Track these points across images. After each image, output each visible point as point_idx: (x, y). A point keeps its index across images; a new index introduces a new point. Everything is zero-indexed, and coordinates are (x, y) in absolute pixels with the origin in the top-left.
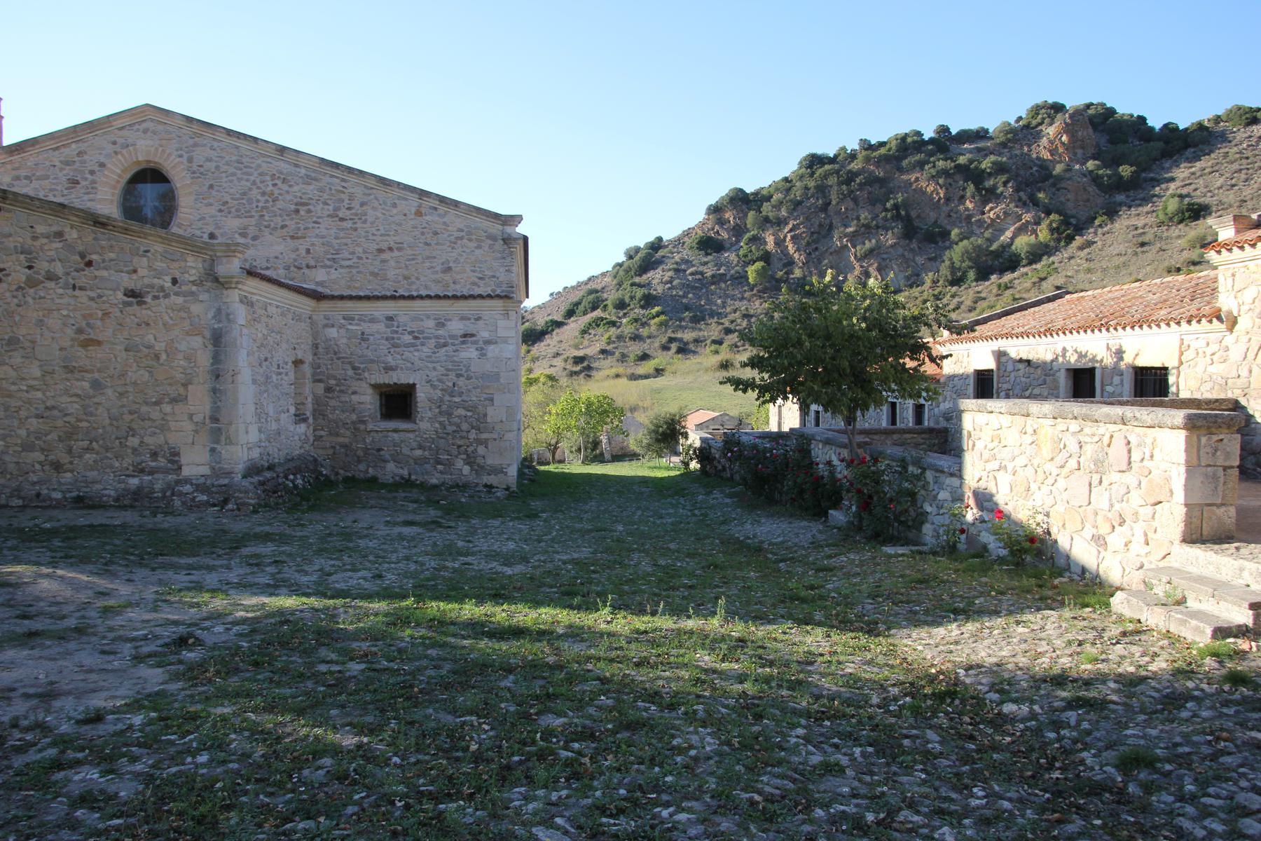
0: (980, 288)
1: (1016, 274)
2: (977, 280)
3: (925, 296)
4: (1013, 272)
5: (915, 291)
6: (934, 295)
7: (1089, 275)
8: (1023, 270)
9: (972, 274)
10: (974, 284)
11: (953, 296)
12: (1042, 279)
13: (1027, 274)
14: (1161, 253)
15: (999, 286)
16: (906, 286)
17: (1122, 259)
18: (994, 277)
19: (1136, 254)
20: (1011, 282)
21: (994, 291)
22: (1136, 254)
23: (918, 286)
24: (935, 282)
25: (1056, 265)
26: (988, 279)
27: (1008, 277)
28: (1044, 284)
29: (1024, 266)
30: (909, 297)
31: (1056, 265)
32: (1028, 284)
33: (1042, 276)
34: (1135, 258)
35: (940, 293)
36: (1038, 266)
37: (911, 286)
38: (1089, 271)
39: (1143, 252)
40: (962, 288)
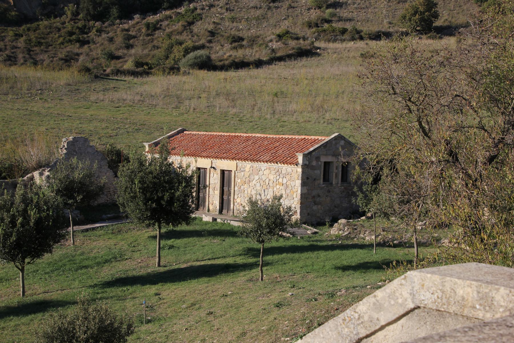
0: (126, 26)
1: (158, 17)
2: (120, 18)
3: (69, 26)
4: (155, 14)
5: (57, 22)
6: (78, 28)
7: (235, 24)
8: (168, 13)
9: (114, 11)
10: (118, 21)
11: (100, 31)
12: (191, 24)
13: (171, 17)
14: (290, 10)
15: (148, 26)
16: (42, 15)
17: (259, 12)
18: (137, 17)
19: (269, 8)
20: (158, 22)
21: (144, 30)
22: (269, 8)
23: (55, 17)
24: (76, 14)
25: (198, 11)
26: (132, 19)
27: (151, 19)
28: (195, 28)
29: (165, 9)
30: (50, 28)
31: (198, 11)
32: (178, 26)
33: (190, 19)
34: (269, 13)
35: (85, 26)
36: (182, 10)
37: (48, 16)
38: (233, 20)
39: (276, 8)
40: (106, 24)
